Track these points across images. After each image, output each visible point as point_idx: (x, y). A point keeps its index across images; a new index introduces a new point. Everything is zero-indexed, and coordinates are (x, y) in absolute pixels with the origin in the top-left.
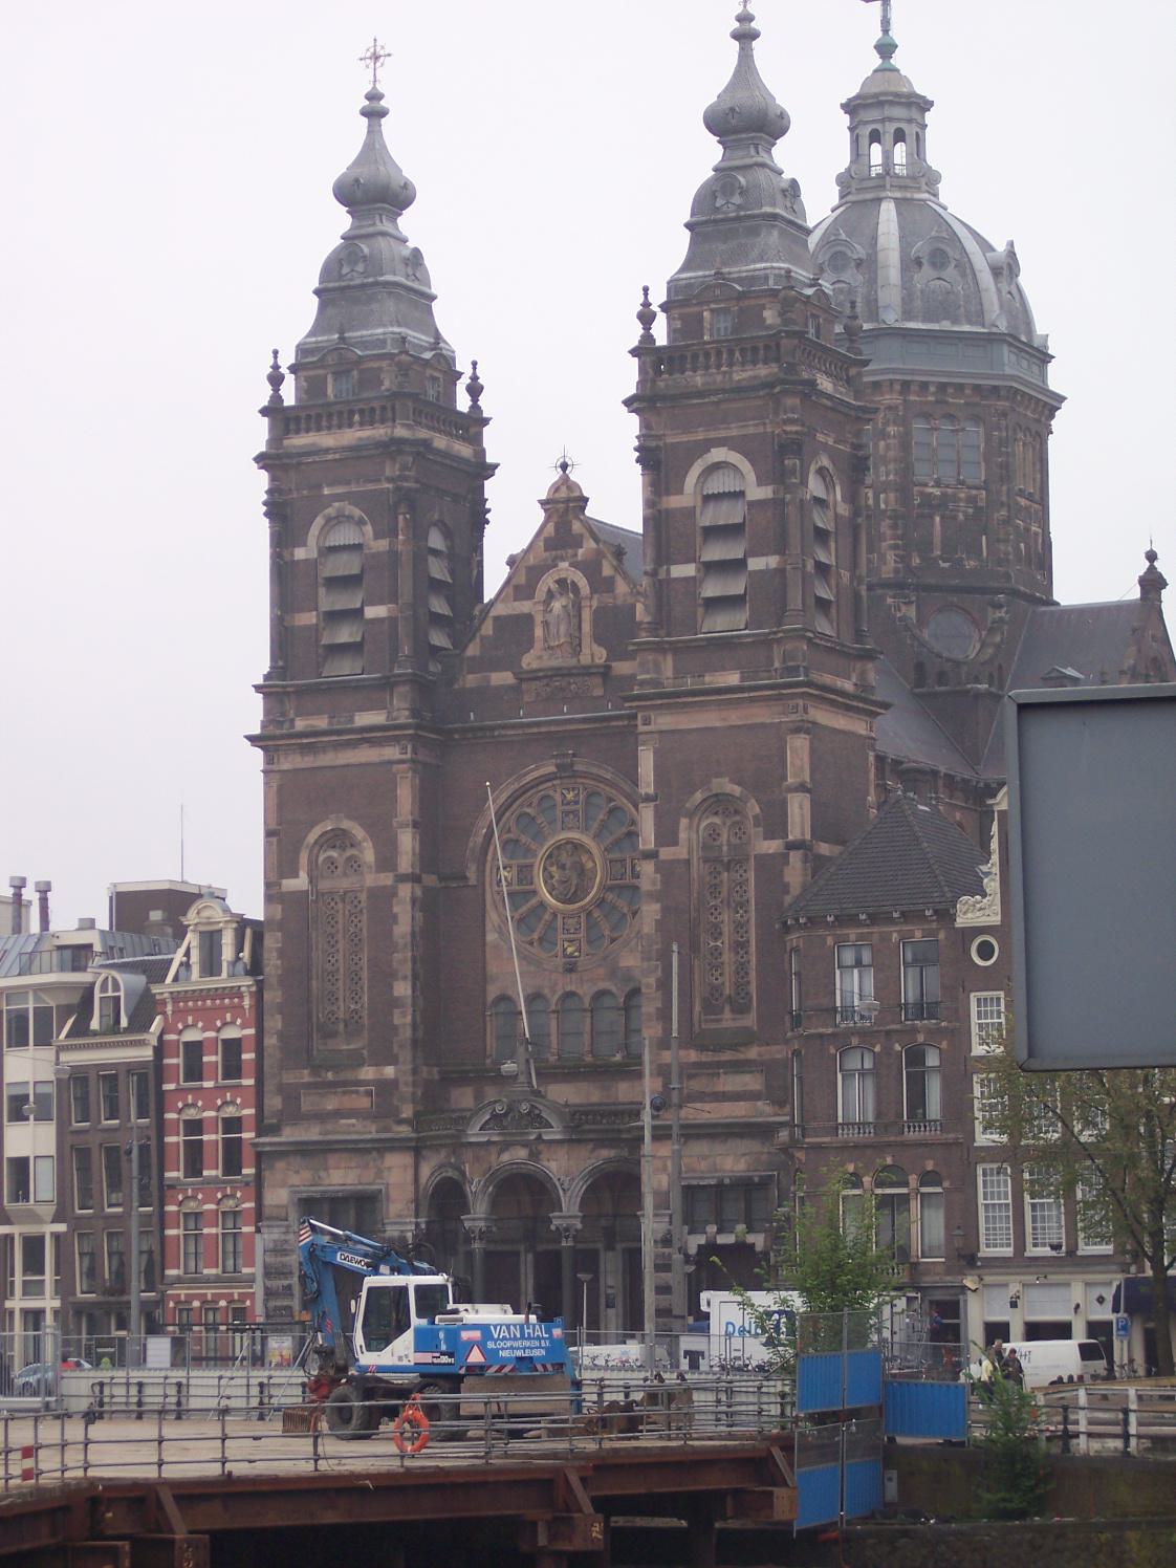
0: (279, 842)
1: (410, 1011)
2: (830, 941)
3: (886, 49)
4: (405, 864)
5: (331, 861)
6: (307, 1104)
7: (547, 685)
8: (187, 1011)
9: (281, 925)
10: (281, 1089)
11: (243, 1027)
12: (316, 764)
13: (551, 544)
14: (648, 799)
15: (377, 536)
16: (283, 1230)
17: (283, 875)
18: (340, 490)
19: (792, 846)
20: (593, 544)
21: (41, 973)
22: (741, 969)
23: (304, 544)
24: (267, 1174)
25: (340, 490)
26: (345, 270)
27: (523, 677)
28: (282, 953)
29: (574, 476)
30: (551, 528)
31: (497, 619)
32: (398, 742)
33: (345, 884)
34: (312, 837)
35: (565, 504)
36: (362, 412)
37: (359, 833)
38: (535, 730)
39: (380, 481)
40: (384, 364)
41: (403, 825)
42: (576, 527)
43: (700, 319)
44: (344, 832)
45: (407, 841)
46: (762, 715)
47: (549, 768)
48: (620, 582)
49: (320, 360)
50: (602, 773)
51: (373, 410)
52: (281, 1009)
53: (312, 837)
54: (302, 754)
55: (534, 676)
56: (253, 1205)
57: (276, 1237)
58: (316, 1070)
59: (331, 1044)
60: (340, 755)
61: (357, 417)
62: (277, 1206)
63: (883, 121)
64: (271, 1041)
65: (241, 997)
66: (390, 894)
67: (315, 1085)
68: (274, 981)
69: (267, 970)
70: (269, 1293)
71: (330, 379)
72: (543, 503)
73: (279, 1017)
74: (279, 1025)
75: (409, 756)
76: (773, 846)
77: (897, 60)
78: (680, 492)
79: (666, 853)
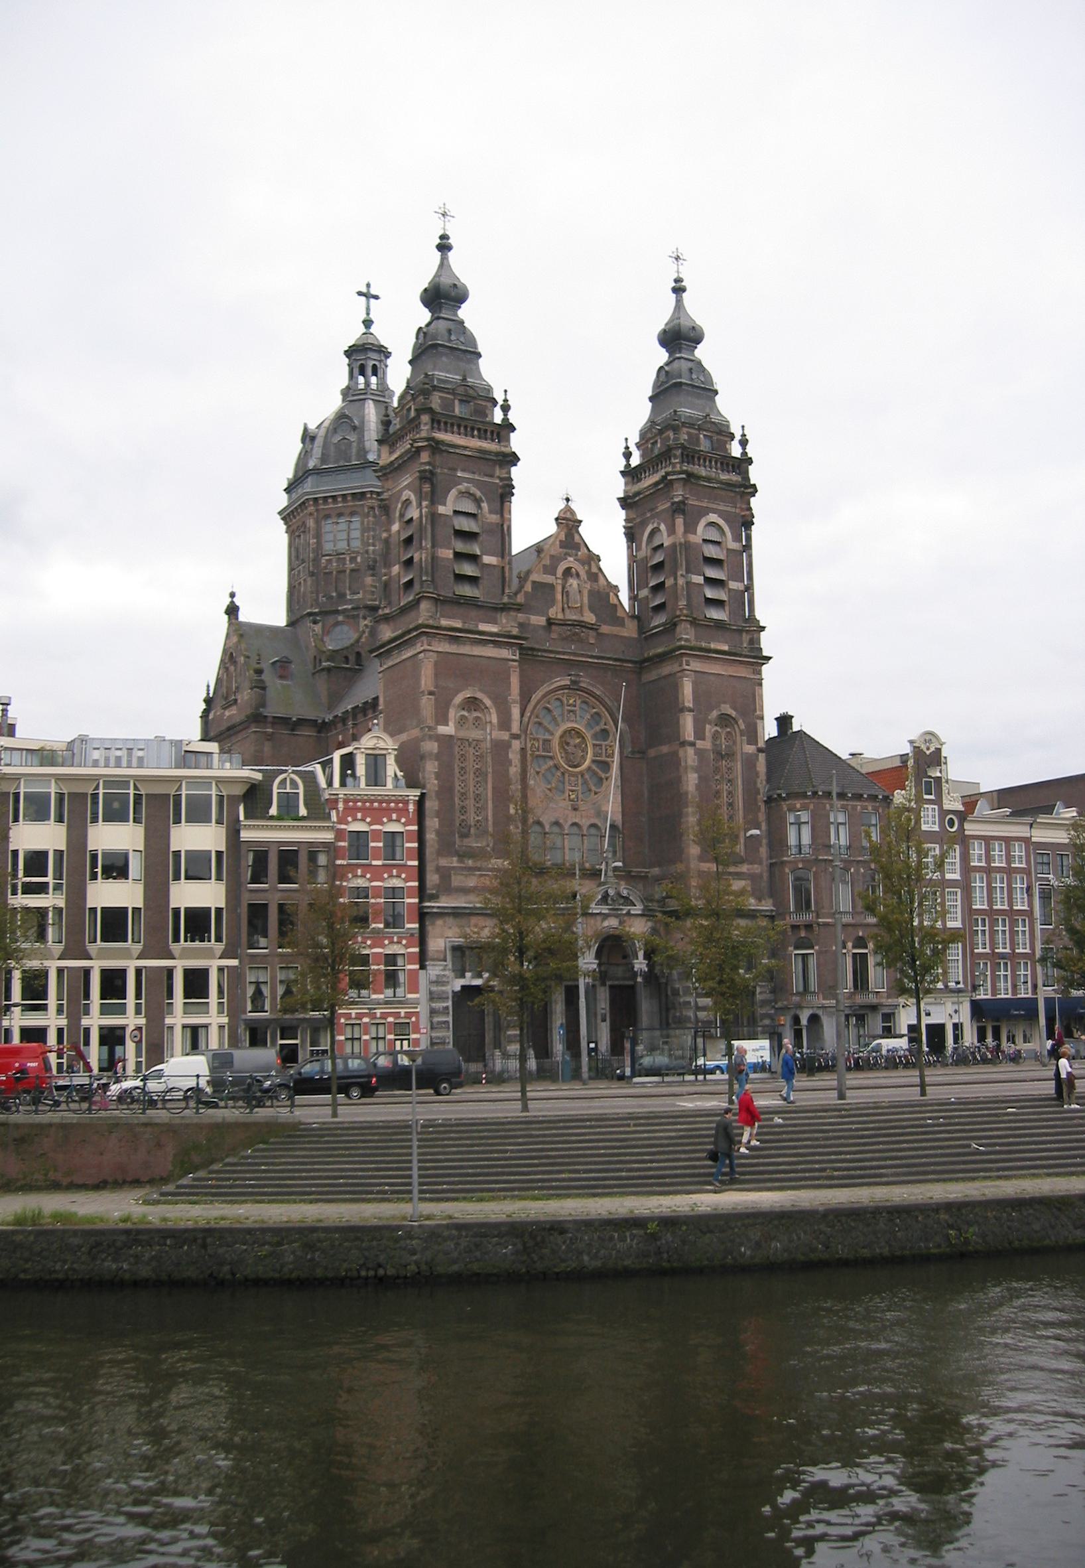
0: (436, 700)
1: (520, 825)
4: (515, 728)
6: (457, 881)
7: (570, 630)
8: (359, 810)
9: (438, 757)
10: (438, 869)
11: (405, 824)
12: (461, 652)
13: (563, 545)
15: (491, 512)
16: (441, 968)
17: (438, 723)
18: (466, 475)
20: (586, 551)
21: (72, 766)
23: (444, 504)
24: (429, 928)
25: (466, 475)
26: (453, 338)
27: (550, 623)
28: (438, 776)
29: (572, 505)
30: (562, 537)
31: (534, 582)
32: (511, 647)
33: (475, 734)
34: (458, 699)
35: (568, 522)
36: (479, 430)
37: (488, 702)
38: (552, 656)
39: (492, 476)
40: (489, 404)
41: (514, 702)
42: (577, 537)
44: (476, 698)
45: (516, 712)
47: (566, 681)
48: (600, 574)
49: (453, 389)
50: (595, 690)
51: (486, 431)
52: (438, 814)
53: (458, 699)
54: (450, 643)
55: (563, 623)
56: (417, 950)
57: (437, 973)
58: (462, 856)
59: (466, 841)
60: (474, 648)
61: (476, 432)
62: (437, 951)
64: (430, 836)
65: (406, 803)
66: (506, 746)
67: (462, 868)
68: (434, 794)
69: (428, 786)
70: (433, 1012)
71: (457, 402)
72: (557, 519)
73: (436, 820)
74: (437, 824)
75: (517, 658)
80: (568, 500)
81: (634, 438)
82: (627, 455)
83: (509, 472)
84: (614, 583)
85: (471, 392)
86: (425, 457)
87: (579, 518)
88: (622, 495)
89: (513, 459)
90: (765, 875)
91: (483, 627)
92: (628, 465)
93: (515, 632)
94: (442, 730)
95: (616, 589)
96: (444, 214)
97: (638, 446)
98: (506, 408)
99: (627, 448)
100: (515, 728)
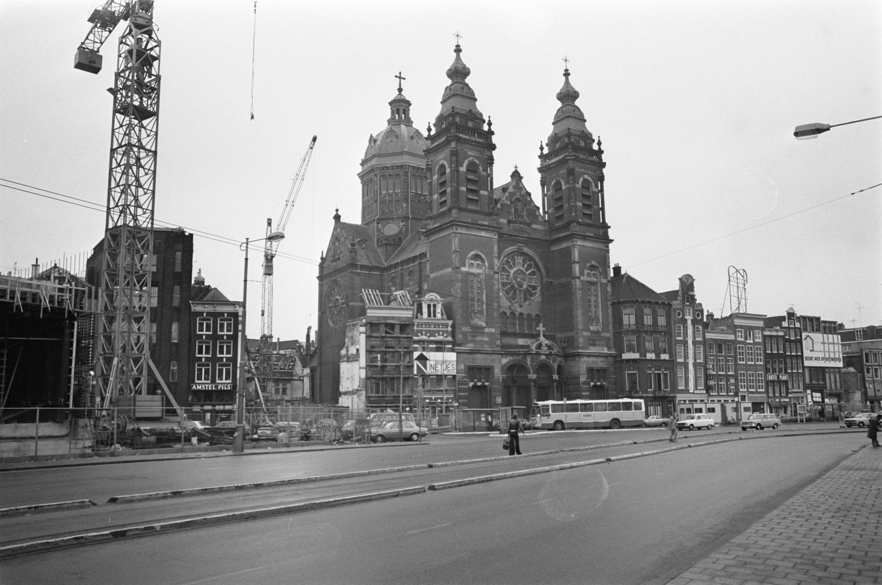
2: (643, 307)
3: (400, 90)
4: (496, 269)
5: (472, 263)
6: (469, 337)
9: (461, 281)
13: (514, 187)
14: (578, 262)
19: (608, 281)
22: (596, 312)
23: (462, 166)
29: (519, 170)
30: (514, 184)
35: (516, 175)
42: (521, 185)
43: (579, 141)
46: (601, 246)
63: (407, 107)
76: (604, 281)
77: (402, 93)
78: (578, 183)
79: (582, 278)
80: (516, 167)
81: (545, 141)
82: (542, 148)
83: (492, 153)
84: (538, 205)
85: (473, 116)
86: (453, 145)
87: (522, 175)
88: (539, 166)
89: (494, 147)
90: (612, 337)
91: (480, 222)
92: (542, 153)
93: (496, 225)
94: (463, 269)
95: (538, 208)
96: (458, 36)
97: (547, 145)
98: (490, 124)
99: (541, 145)
100: (496, 269)
